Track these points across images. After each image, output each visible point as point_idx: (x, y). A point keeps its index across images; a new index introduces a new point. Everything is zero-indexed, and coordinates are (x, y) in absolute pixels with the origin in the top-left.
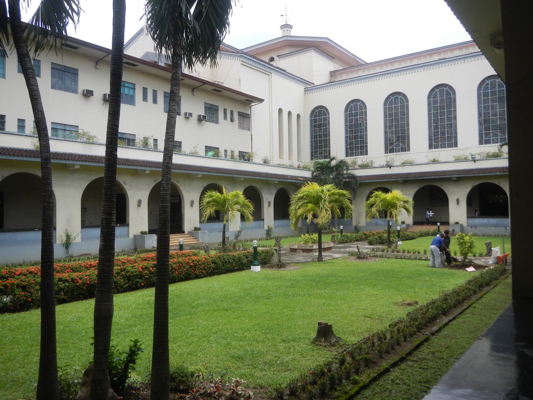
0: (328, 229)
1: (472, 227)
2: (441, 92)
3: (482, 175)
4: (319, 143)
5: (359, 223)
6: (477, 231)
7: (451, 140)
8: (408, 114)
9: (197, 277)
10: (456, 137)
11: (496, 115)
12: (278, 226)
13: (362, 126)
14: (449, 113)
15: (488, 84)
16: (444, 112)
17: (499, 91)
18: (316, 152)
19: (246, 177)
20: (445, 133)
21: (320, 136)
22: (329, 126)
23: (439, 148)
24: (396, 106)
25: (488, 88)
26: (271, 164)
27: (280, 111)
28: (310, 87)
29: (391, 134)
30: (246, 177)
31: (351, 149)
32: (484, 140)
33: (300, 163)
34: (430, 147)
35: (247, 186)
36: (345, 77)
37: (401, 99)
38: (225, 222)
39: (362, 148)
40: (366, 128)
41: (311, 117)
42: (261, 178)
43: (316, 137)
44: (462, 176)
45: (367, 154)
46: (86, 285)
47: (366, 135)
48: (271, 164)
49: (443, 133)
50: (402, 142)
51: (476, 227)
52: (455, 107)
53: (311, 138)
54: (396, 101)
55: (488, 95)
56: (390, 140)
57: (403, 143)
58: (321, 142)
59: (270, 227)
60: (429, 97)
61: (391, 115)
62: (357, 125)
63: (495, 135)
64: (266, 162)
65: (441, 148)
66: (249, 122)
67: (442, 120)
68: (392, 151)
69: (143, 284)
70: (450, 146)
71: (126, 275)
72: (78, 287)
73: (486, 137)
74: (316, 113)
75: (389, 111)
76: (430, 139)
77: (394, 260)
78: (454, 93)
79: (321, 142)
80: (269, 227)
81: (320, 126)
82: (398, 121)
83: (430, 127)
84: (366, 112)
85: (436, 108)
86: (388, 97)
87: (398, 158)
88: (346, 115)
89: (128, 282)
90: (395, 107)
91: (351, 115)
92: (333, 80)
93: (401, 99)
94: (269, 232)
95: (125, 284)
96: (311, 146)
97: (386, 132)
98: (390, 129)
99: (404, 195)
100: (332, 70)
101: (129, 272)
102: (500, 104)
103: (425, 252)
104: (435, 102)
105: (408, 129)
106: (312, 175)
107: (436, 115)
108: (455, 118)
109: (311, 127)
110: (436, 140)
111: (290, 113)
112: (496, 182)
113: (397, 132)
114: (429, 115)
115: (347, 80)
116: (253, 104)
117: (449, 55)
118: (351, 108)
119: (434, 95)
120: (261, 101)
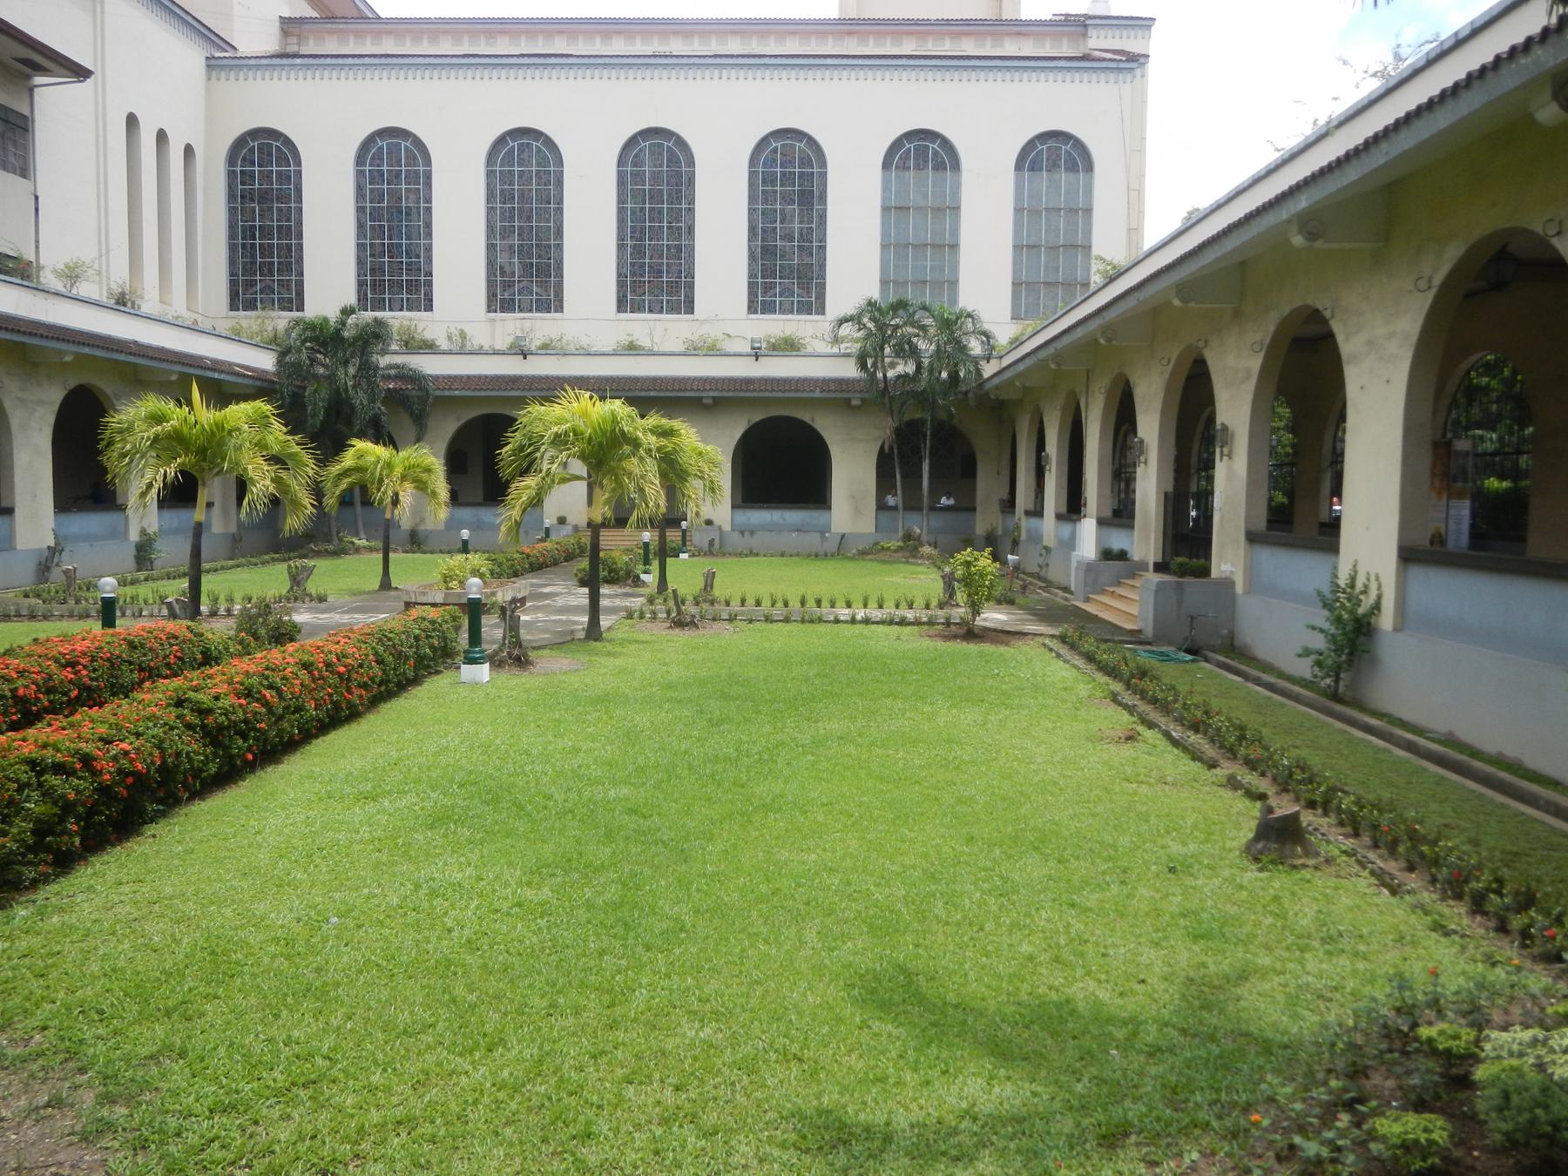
0: (336, 541)
1: (742, 533)
2: (656, 151)
3: (780, 395)
4: (262, 255)
5: (422, 520)
6: (754, 542)
7: (678, 293)
8: (560, 202)
9: (354, 715)
10: (690, 287)
11: (789, 237)
12: (175, 532)
13: (414, 216)
14: (676, 215)
15: (775, 151)
16: (660, 211)
17: (801, 175)
18: (250, 284)
19: (87, 350)
20: (661, 271)
21: (266, 232)
22: (299, 199)
24: (524, 172)
25: (775, 160)
26: (146, 308)
27: (132, 121)
28: (222, 58)
29: (505, 255)
30: (87, 350)
31: (377, 286)
32: (761, 300)
33: (195, 316)
34: (621, 306)
35: (72, 384)
36: (331, 46)
37: (539, 150)
38: (199, 514)
39: (413, 286)
40: (429, 225)
41: (232, 159)
42: (131, 359)
43: (250, 233)
44: (730, 394)
45: (429, 307)
46: (130, 780)
47: (429, 249)
48: (146, 308)
49: (655, 270)
50: (540, 284)
51: (752, 533)
52: (692, 201)
53: (232, 235)
54: (525, 155)
55: (773, 183)
56: (503, 273)
57: (544, 285)
58: (266, 251)
59: (150, 531)
60: (621, 162)
61: (507, 197)
62: (396, 212)
64: (122, 302)
65: (651, 311)
66: (25, 148)
67: (656, 233)
68: (507, 306)
69: (250, 757)
70: (674, 309)
71: (203, 727)
72: (104, 790)
73: (765, 293)
74: (252, 150)
75: (503, 182)
76: (621, 284)
77: (764, 625)
79: (266, 251)
80: (143, 532)
81: (264, 197)
82: (529, 219)
83: (621, 247)
84: (428, 176)
85: (639, 196)
86: (501, 141)
87: (540, 327)
88: (360, 174)
89: (215, 755)
90: (521, 174)
91: (377, 177)
92: (292, 49)
93: (539, 150)
94: (144, 554)
95: (206, 762)
96: (232, 262)
97: (491, 248)
98: (503, 238)
99: (705, 440)
100: (286, 14)
101: (210, 711)
103: (803, 603)
104: (638, 177)
105: (560, 247)
106: (280, 362)
107: (638, 215)
108: (691, 230)
109: (231, 196)
110: (637, 286)
111: (162, 136)
112: (805, 416)
113: (524, 252)
115: (367, 60)
116: (38, 80)
117: (676, 46)
118: (378, 157)
120: (80, 73)
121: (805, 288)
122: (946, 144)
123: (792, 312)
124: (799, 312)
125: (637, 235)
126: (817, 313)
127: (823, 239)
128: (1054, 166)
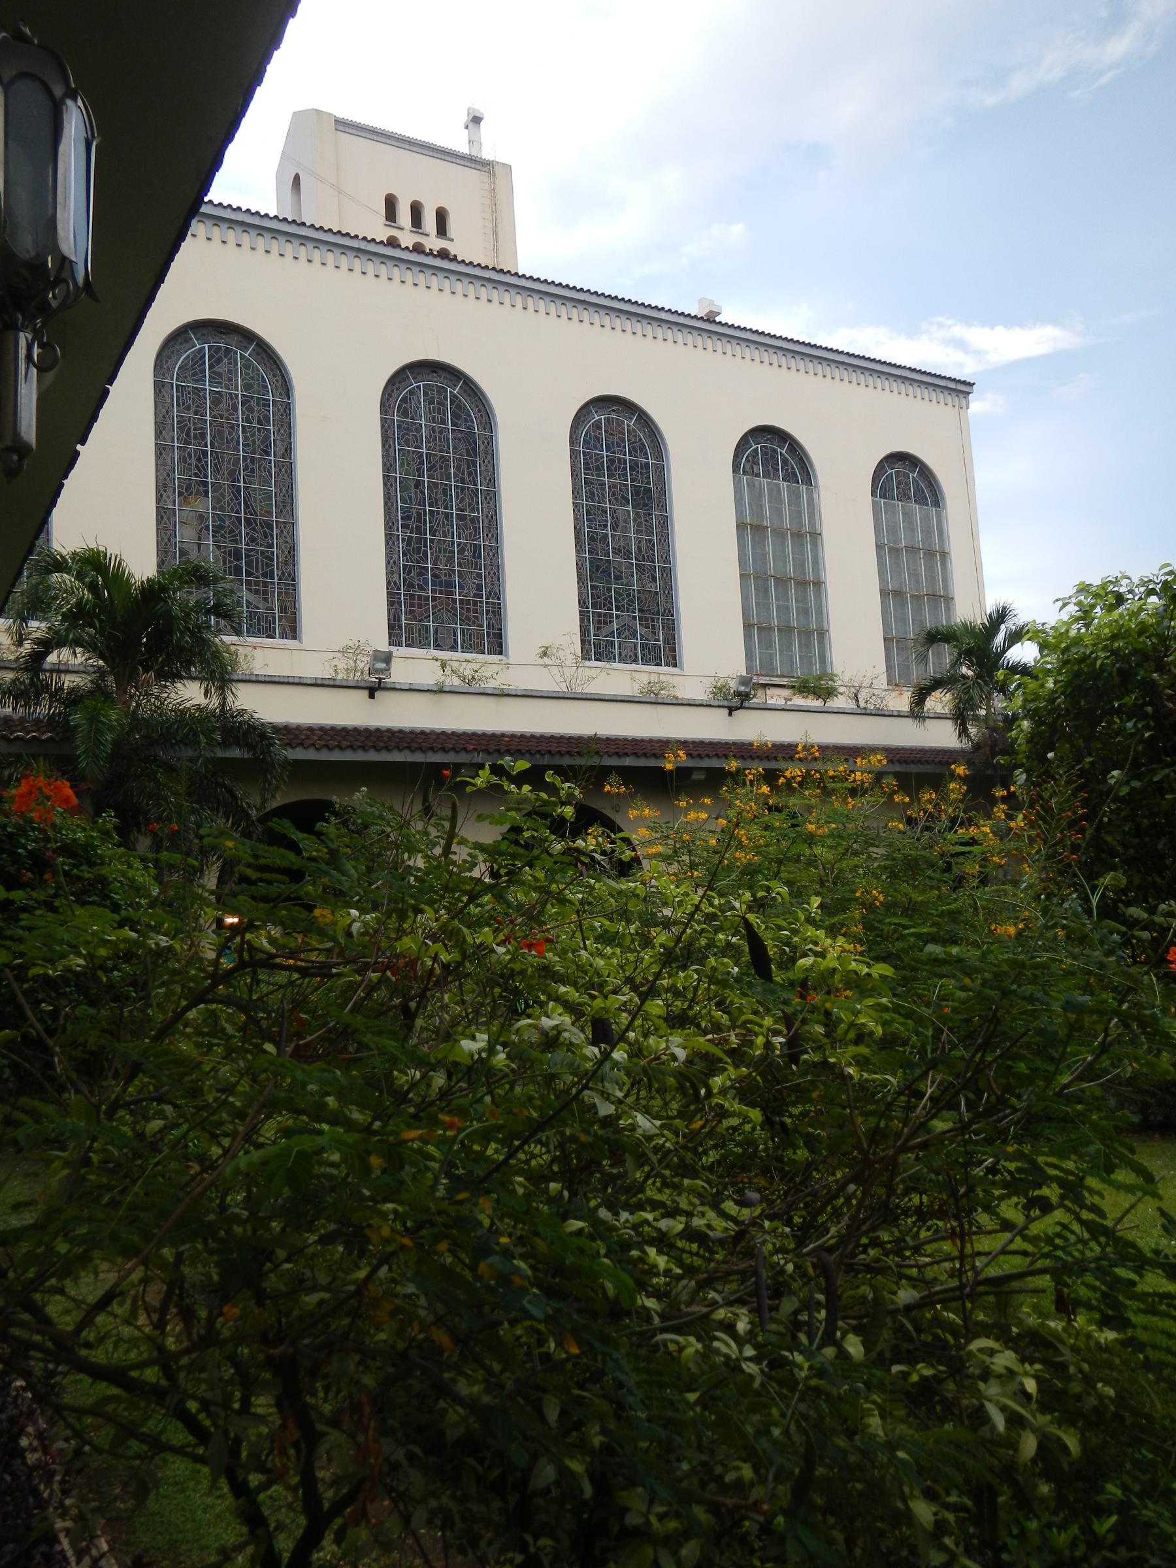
7: (477, 620)
10: (497, 612)
14: (469, 497)
15: (597, 426)
20: (449, 584)
23: (426, 646)
25: (598, 439)
37: (247, 366)
54: (222, 368)
60: (385, 406)
61: (191, 433)
63: (627, 631)
78: (488, 422)
97: (163, 516)
102: (637, 514)
104: (409, 433)
105: (289, 528)
110: (416, 605)
114: (387, 481)
119: (404, 400)
121: (649, 623)
122: (795, 447)
123: (635, 661)
124: (646, 661)
125: (413, 523)
126: (668, 665)
127: (667, 558)
128: (904, 496)
